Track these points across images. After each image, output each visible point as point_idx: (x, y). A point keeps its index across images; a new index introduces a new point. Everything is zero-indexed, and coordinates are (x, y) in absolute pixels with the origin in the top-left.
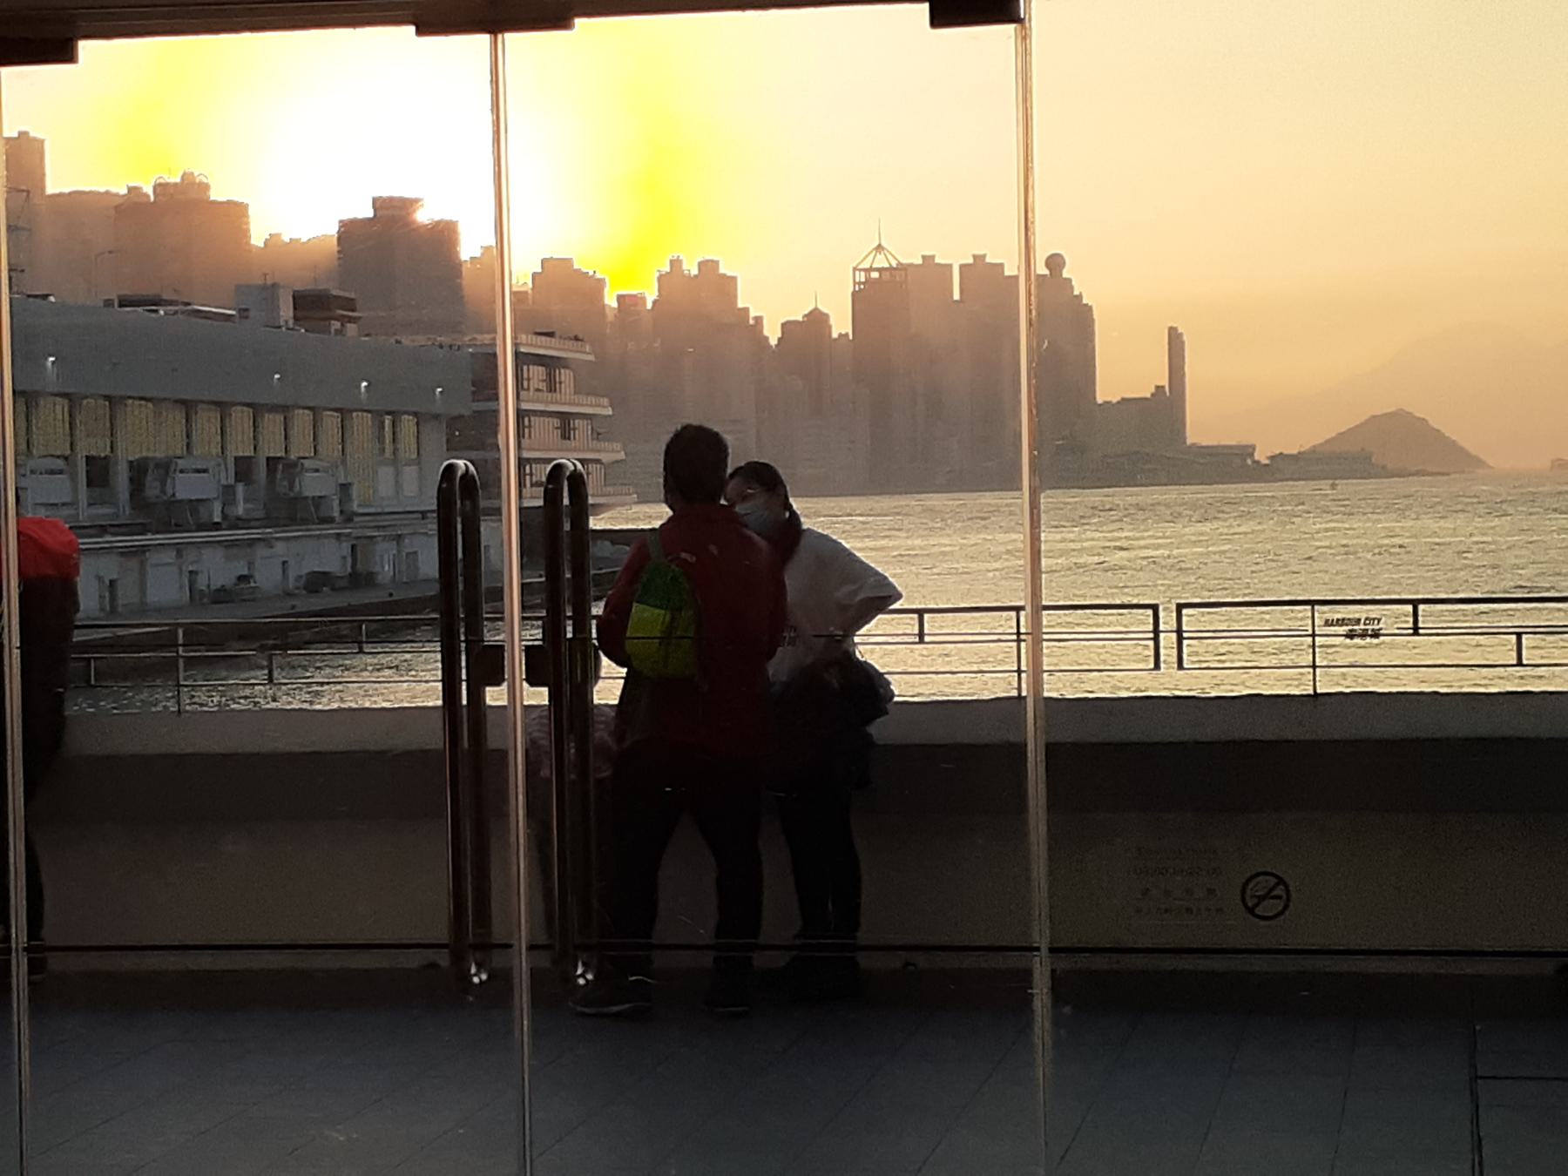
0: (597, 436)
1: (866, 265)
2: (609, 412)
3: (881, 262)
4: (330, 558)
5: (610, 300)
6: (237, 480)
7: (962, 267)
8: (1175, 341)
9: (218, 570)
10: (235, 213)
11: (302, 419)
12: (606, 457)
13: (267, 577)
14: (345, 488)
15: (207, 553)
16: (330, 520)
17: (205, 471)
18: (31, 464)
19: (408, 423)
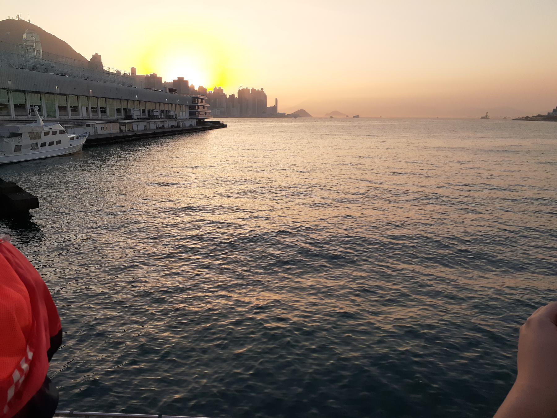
0: (208, 109)
3: (241, 88)
4: (174, 123)
5: (208, 92)
9: (160, 125)
11: (170, 105)
12: (209, 112)
14: (176, 114)
16: (174, 119)
18: (134, 110)
19: (184, 106)
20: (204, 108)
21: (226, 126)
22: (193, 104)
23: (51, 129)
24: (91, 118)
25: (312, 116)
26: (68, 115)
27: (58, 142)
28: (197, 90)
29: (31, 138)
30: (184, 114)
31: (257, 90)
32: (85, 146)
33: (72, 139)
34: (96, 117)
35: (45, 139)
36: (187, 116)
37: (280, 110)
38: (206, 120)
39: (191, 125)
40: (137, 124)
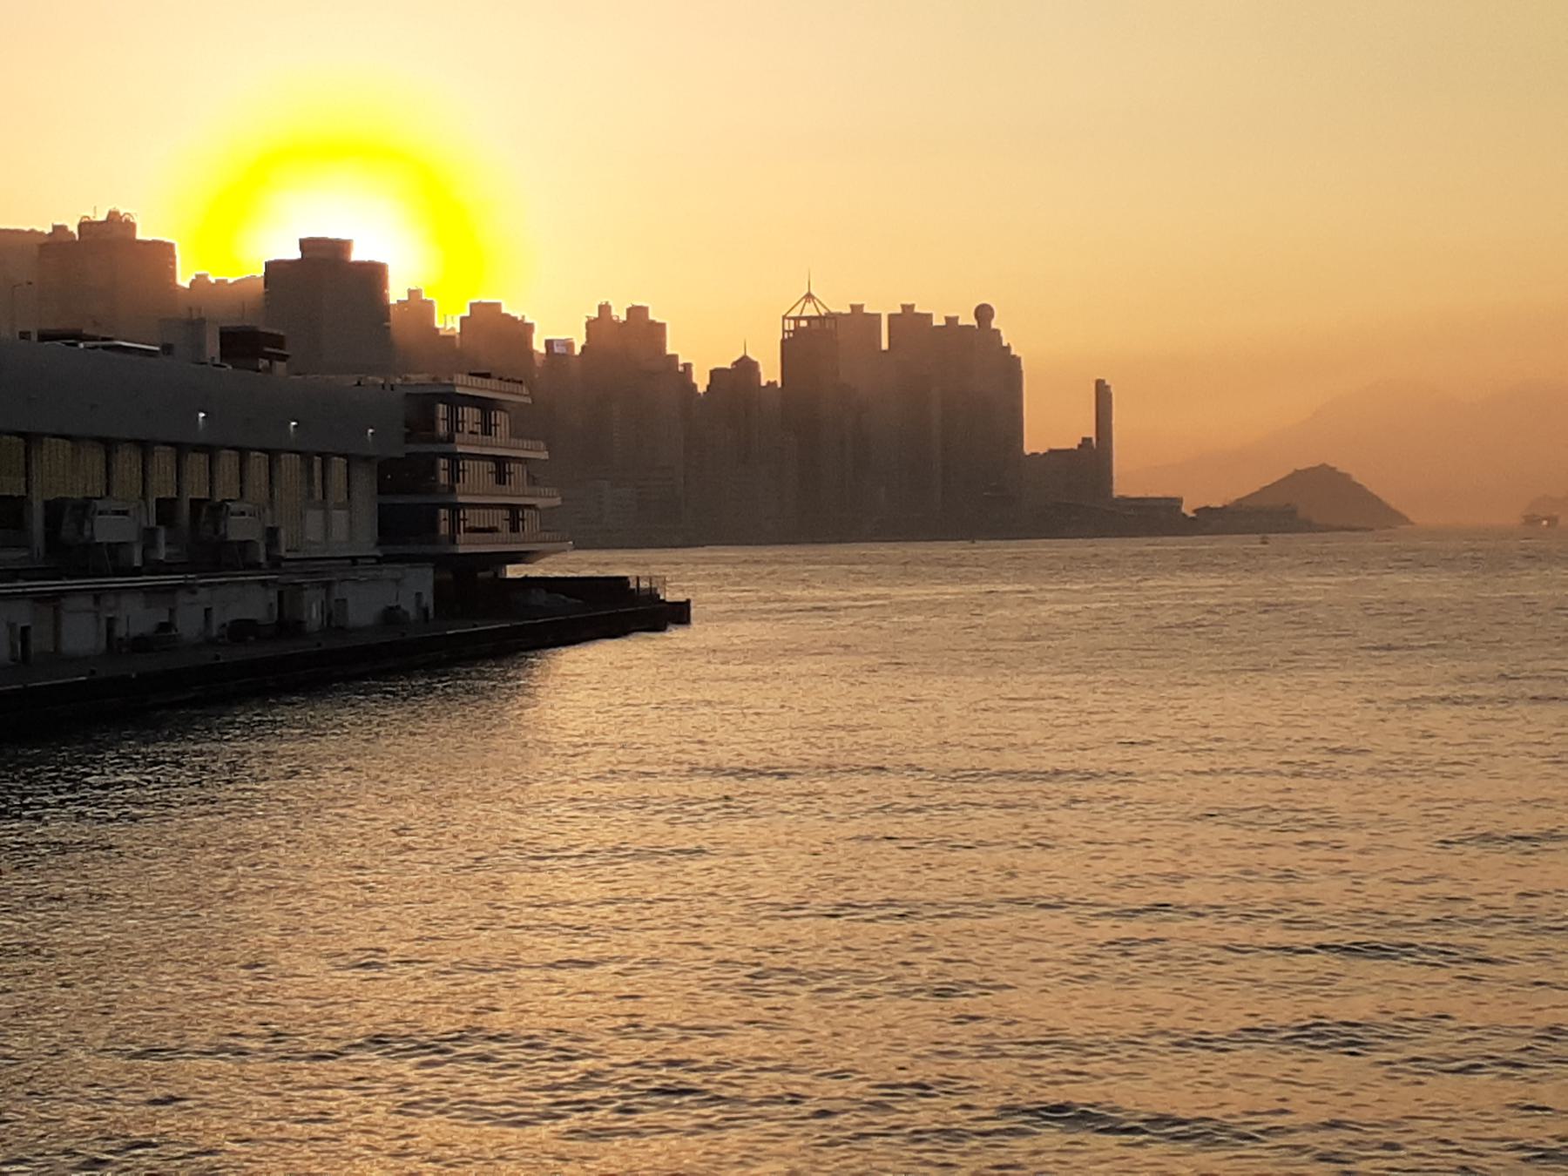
0: (533, 480)
1: (795, 313)
2: (544, 455)
3: (810, 310)
5: (539, 346)
6: (158, 523)
7: (891, 317)
9: (137, 618)
10: (162, 252)
11: (228, 462)
12: (540, 503)
13: (189, 624)
14: (272, 533)
17: (125, 513)
19: (338, 464)
20: (501, 477)
21: (679, 614)
22: (413, 448)
25: (1412, 518)
28: (452, 337)
31: (939, 321)
36: (366, 543)
38: (513, 572)
39: (391, 616)
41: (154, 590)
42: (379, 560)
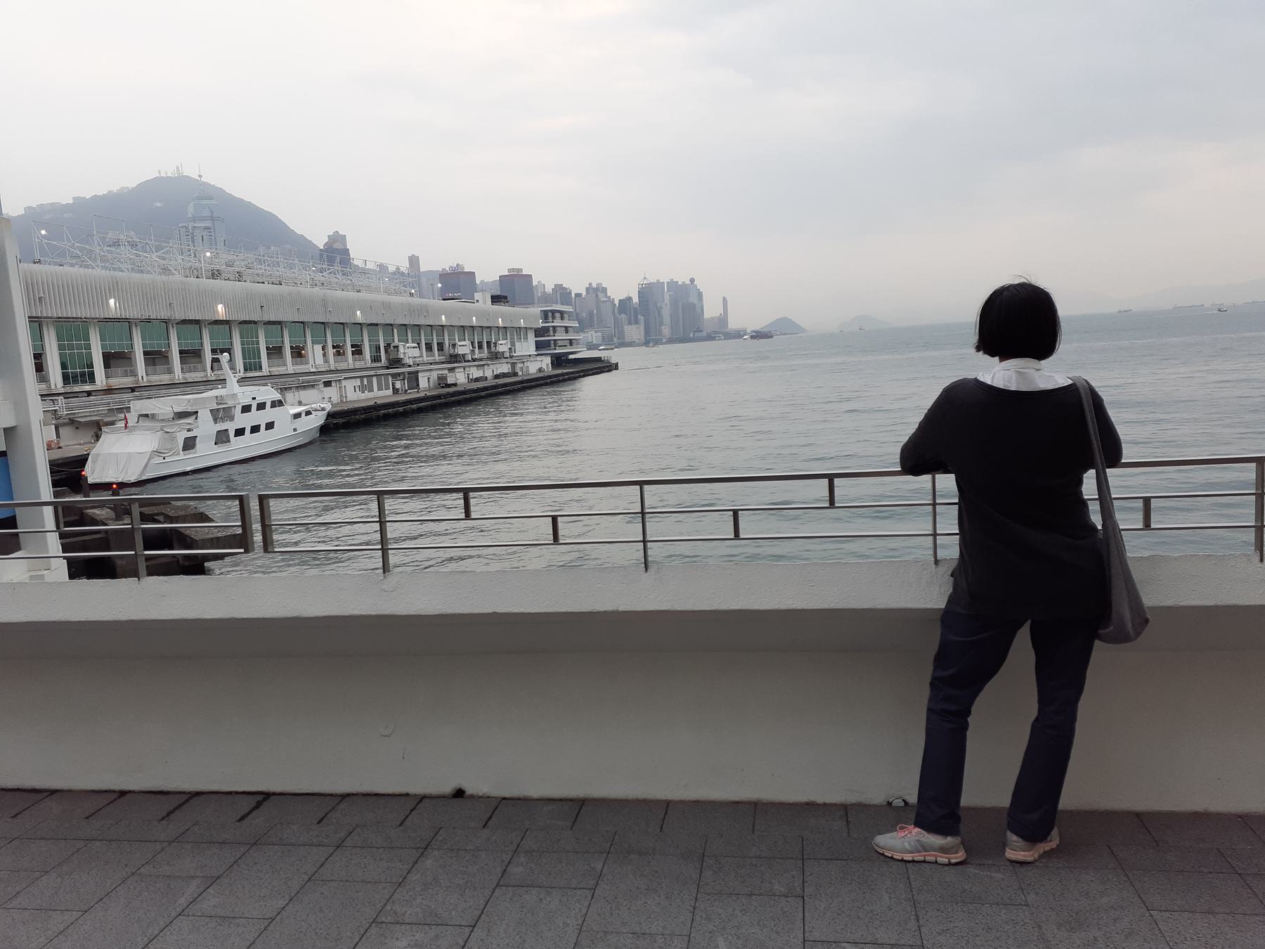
3: (645, 282)
4: (505, 368)
7: (667, 283)
8: (724, 299)
9: (476, 373)
15: (472, 368)
23: (254, 398)
24: (333, 368)
26: (285, 365)
27: (270, 426)
29: (215, 420)
30: (527, 347)
32: (324, 429)
33: (297, 416)
34: (343, 366)
35: (245, 421)
37: (733, 324)
38: (571, 357)
39: (540, 370)
40: (427, 374)
41: (478, 366)
42: (536, 355)
